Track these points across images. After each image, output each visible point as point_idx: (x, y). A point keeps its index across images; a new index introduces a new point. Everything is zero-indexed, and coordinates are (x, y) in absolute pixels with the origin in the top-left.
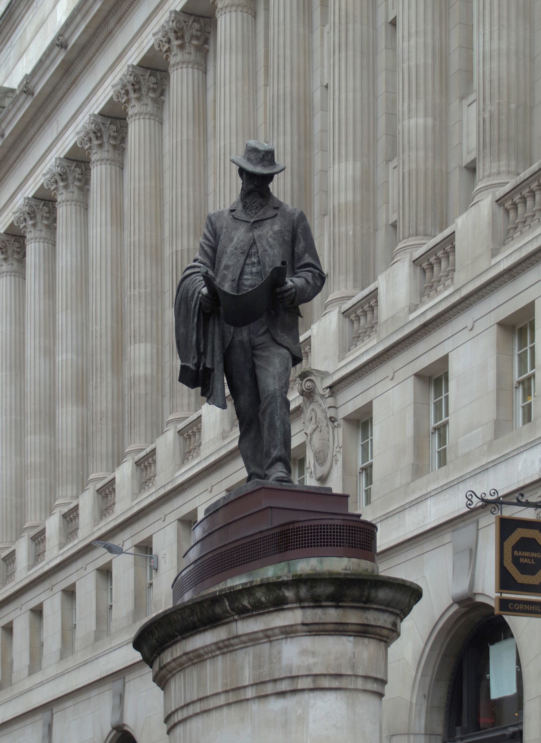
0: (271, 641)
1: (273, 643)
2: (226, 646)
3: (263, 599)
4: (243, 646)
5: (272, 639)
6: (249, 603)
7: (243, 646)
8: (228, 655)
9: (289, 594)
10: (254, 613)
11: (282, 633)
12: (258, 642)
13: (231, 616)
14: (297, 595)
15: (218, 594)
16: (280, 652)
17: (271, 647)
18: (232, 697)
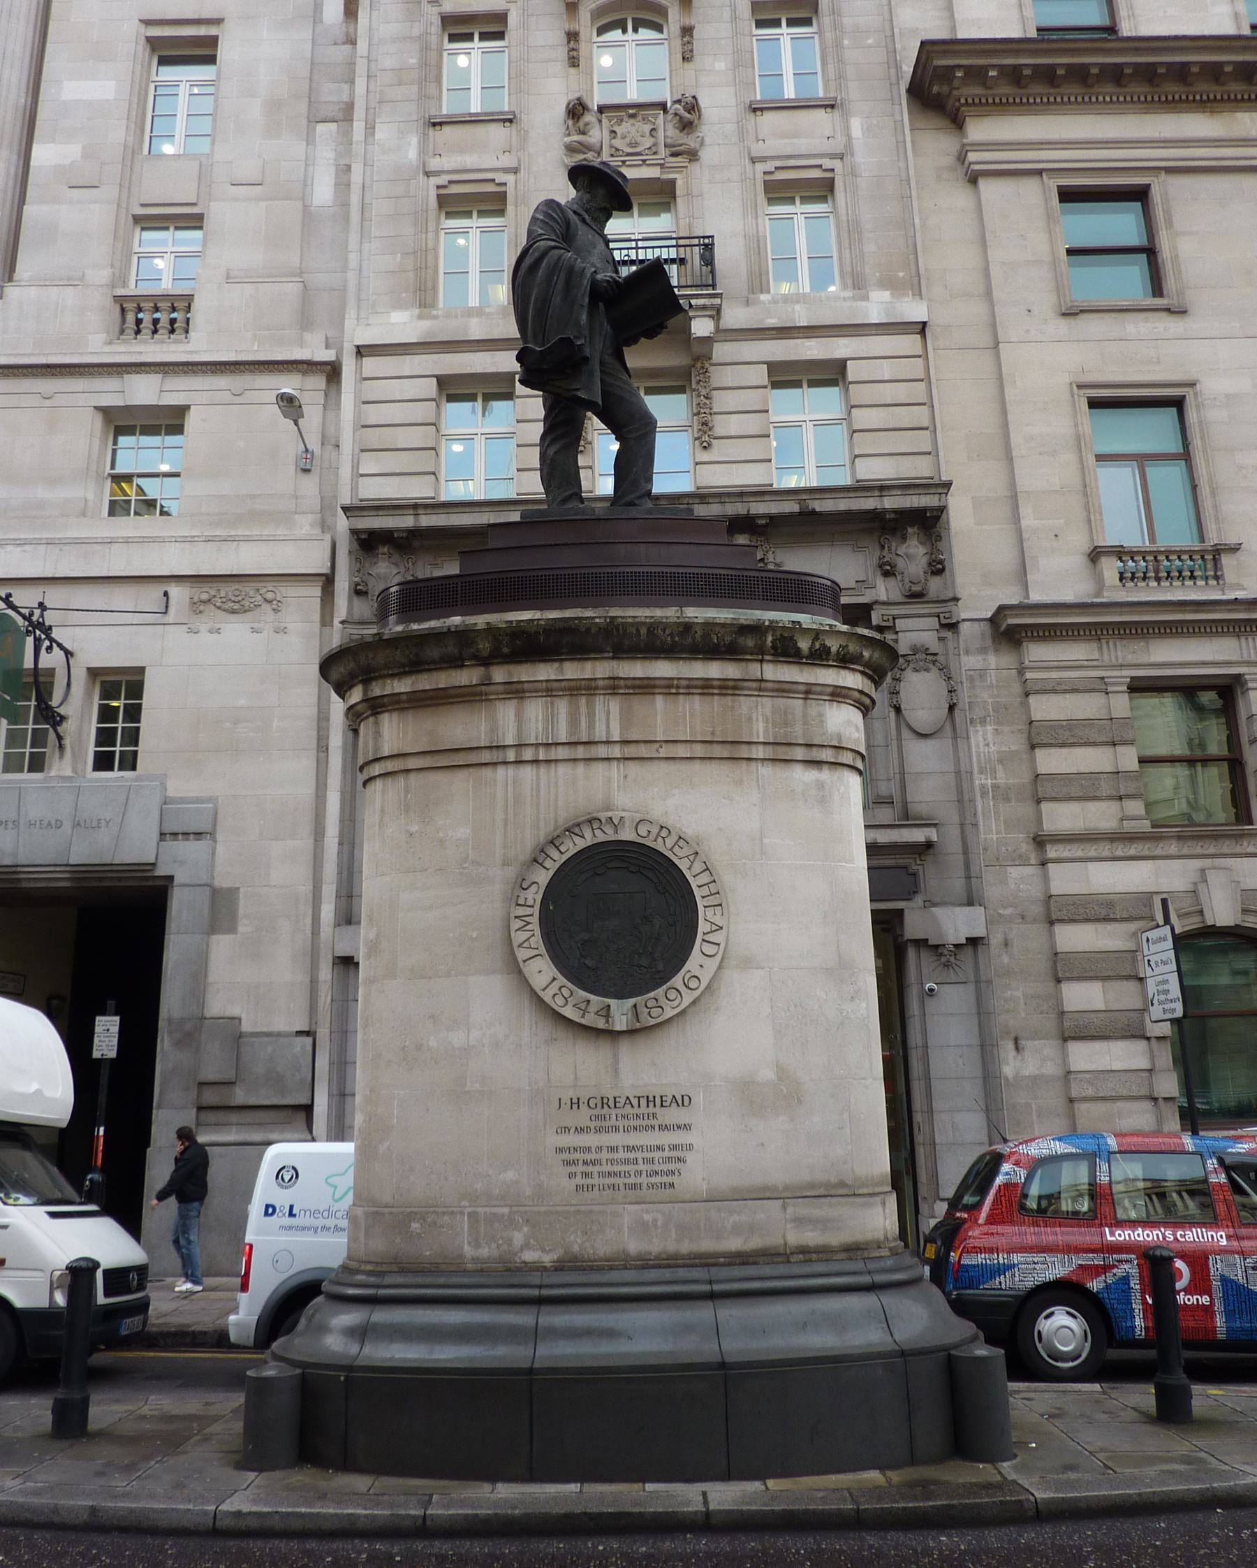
0: (805, 699)
1: (808, 701)
2: (720, 687)
3: (834, 649)
4: (756, 693)
5: (811, 696)
6: (810, 649)
7: (756, 693)
8: (716, 698)
9: (866, 654)
10: (804, 660)
11: (832, 694)
12: (785, 695)
13: (757, 654)
14: (871, 657)
15: (767, 623)
16: (821, 715)
17: (805, 704)
18: (718, 751)
